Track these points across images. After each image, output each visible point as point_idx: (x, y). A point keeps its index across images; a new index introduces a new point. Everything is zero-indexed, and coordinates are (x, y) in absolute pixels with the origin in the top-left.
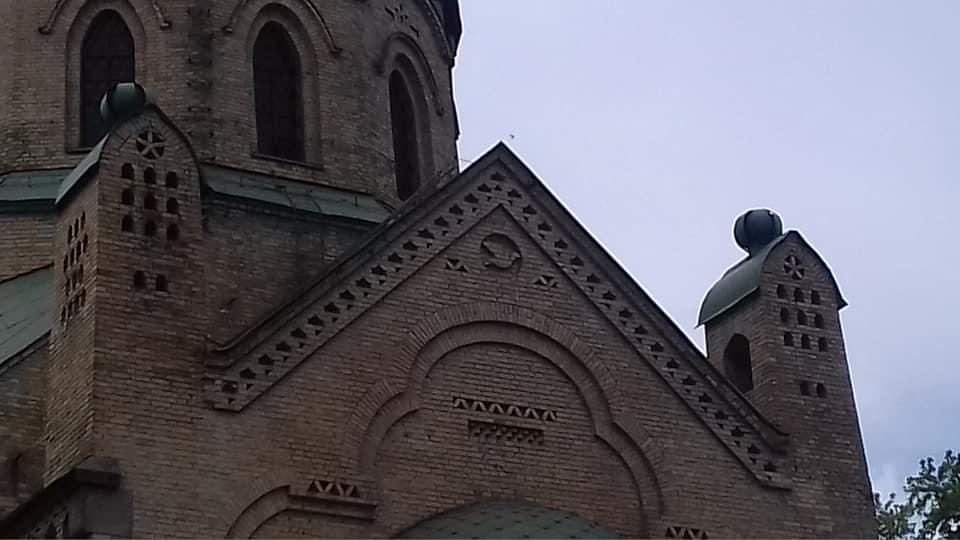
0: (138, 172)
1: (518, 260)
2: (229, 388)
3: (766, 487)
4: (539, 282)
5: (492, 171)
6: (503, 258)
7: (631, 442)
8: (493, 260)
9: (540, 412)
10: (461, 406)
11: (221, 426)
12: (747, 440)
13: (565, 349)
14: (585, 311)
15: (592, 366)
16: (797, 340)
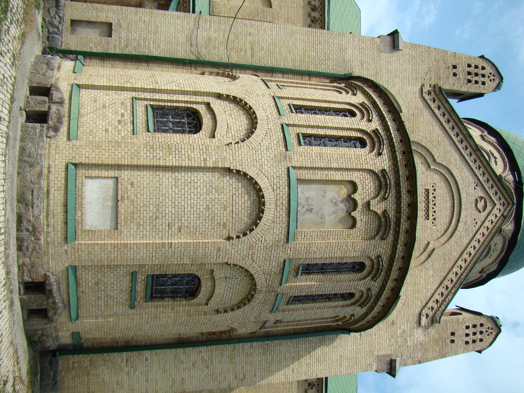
0: (483, 72)
1: (480, 212)
2: (429, 93)
3: (420, 314)
4: (475, 220)
5: (505, 202)
6: (481, 205)
7: (429, 256)
8: (479, 201)
9: (434, 219)
10: (433, 186)
11: (417, 89)
12: (435, 306)
13: (455, 229)
14: (469, 238)
15: (452, 239)
16: (467, 331)
